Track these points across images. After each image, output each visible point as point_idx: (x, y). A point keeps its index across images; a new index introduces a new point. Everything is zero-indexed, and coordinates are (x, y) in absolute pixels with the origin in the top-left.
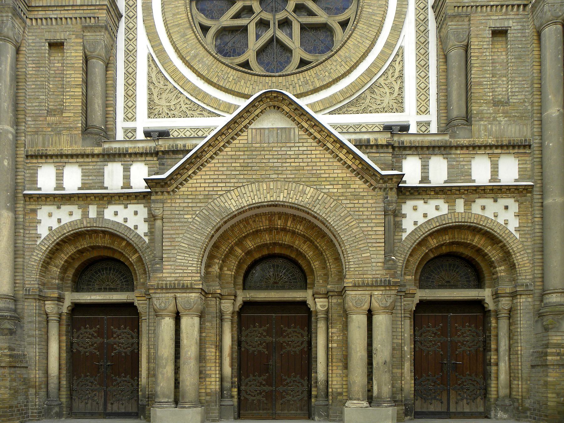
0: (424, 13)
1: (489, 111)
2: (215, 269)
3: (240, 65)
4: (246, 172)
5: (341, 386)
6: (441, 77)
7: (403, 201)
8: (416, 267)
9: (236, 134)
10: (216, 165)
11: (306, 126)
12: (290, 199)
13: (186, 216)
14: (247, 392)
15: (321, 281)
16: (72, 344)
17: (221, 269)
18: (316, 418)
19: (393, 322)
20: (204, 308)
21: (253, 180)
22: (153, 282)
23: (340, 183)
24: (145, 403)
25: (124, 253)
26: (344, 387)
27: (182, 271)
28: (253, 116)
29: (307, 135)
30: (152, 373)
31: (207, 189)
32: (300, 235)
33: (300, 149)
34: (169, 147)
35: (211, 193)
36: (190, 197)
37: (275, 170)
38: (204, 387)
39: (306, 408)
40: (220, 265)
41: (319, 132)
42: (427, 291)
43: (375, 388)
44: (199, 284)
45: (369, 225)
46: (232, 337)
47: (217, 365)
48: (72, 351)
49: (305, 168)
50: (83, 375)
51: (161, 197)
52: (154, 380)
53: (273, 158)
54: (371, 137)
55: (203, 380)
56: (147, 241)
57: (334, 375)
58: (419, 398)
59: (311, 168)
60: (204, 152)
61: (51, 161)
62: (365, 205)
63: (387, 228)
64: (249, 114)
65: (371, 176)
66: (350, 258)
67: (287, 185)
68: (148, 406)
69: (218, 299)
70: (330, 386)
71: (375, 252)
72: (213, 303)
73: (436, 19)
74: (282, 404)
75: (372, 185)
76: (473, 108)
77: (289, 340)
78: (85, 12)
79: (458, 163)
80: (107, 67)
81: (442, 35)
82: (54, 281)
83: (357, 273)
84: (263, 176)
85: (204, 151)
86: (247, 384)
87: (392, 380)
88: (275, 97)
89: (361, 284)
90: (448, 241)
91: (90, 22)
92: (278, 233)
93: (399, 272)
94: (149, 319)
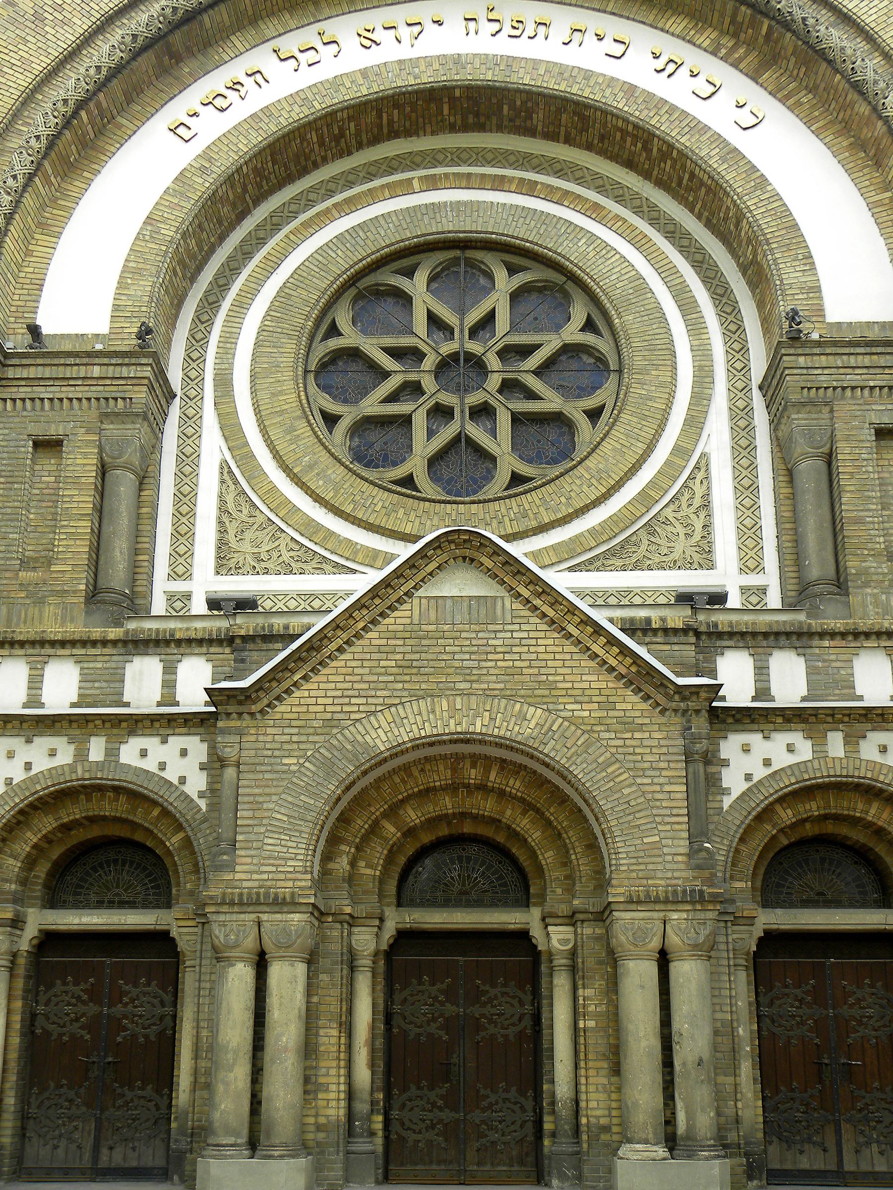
0: (744, 397)
1: (880, 570)
2: (342, 864)
3: (395, 482)
4: (407, 678)
5: (606, 1112)
6: (783, 508)
7: (722, 734)
8: (753, 863)
9: (389, 608)
10: (349, 664)
11: (526, 593)
12: (496, 730)
13: (285, 761)
14: (403, 1124)
15: (559, 891)
16: (33, 1016)
17: (353, 864)
18: (555, 1182)
19: (714, 976)
20: (317, 944)
21: (421, 693)
22: (214, 891)
23: (595, 699)
24: (183, 1146)
25: (155, 831)
26: (614, 1113)
27: (274, 869)
28: (422, 574)
29: (529, 609)
30: (203, 1080)
32: (515, 797)
33: (515, 635)
34: (255, 629)
36: (294, 723)
37: (466, 673)
38: (313, 1112)
39: (531, 1159)
40: (350, 857)
41: (551, 605)
42: (779, 911)
43: (681, 1117)
44: (308, 896)
45: (656, 780)
46: (374, 1005)
47: (342, 1063)
48: (33, 1032)
49: (525, 671)
50: (52, 1085)
51: (238, 723)
52: (206, 1096)
53: (461, 652)
54: (654, 615)
55: (311, 1096)
56: (204, 808)
57: (592, 1088)
58: (774, 1138)
59: (536, 671)
60: (325, 640)
61: (21, 652)
62: (645, 743)
63: (692, 786)
64: (414, 571)
65: (656, 687)
66: (619, 845)
67: (489, 702)
68: (191, 1153)
69: (346, 926)
70: (583, 1112)
71: (669, 834)
72: (336, 933)
73: (767, 407)
74: (478, 1151)
75: (658, 704)
76: (849, 564)
77: (494, 1011)
78: (107, 388)
79: (826, 664)
80: (141, 483)
81: (780, 434)
82: (7, 886)
83: (634, 875)
84: (441, 685)
85: (326, 636)
86: (404, 1105)
87: (717, 1100)
88: (465, 541)
89: (642, 898)
90: (816, 813)
91: (116, 406)
92: (470, 793)
93: (719, 874)
94: (200, 965)
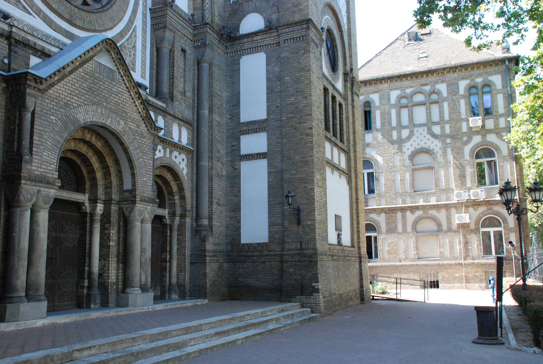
11: (122, 74)
31: (67, 98)
35: (69, 102)
41: (128, 81)
